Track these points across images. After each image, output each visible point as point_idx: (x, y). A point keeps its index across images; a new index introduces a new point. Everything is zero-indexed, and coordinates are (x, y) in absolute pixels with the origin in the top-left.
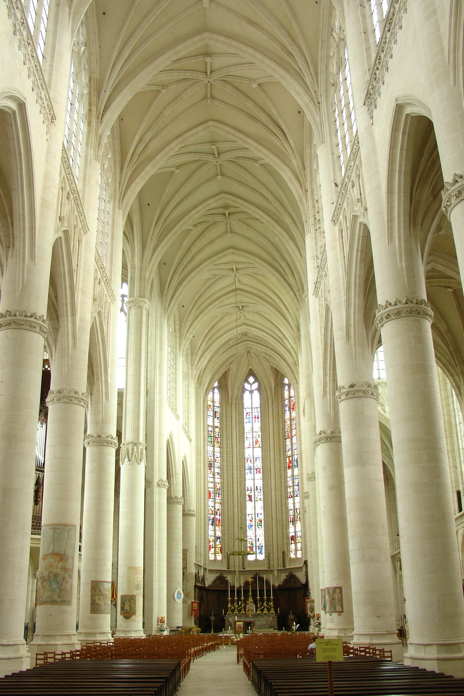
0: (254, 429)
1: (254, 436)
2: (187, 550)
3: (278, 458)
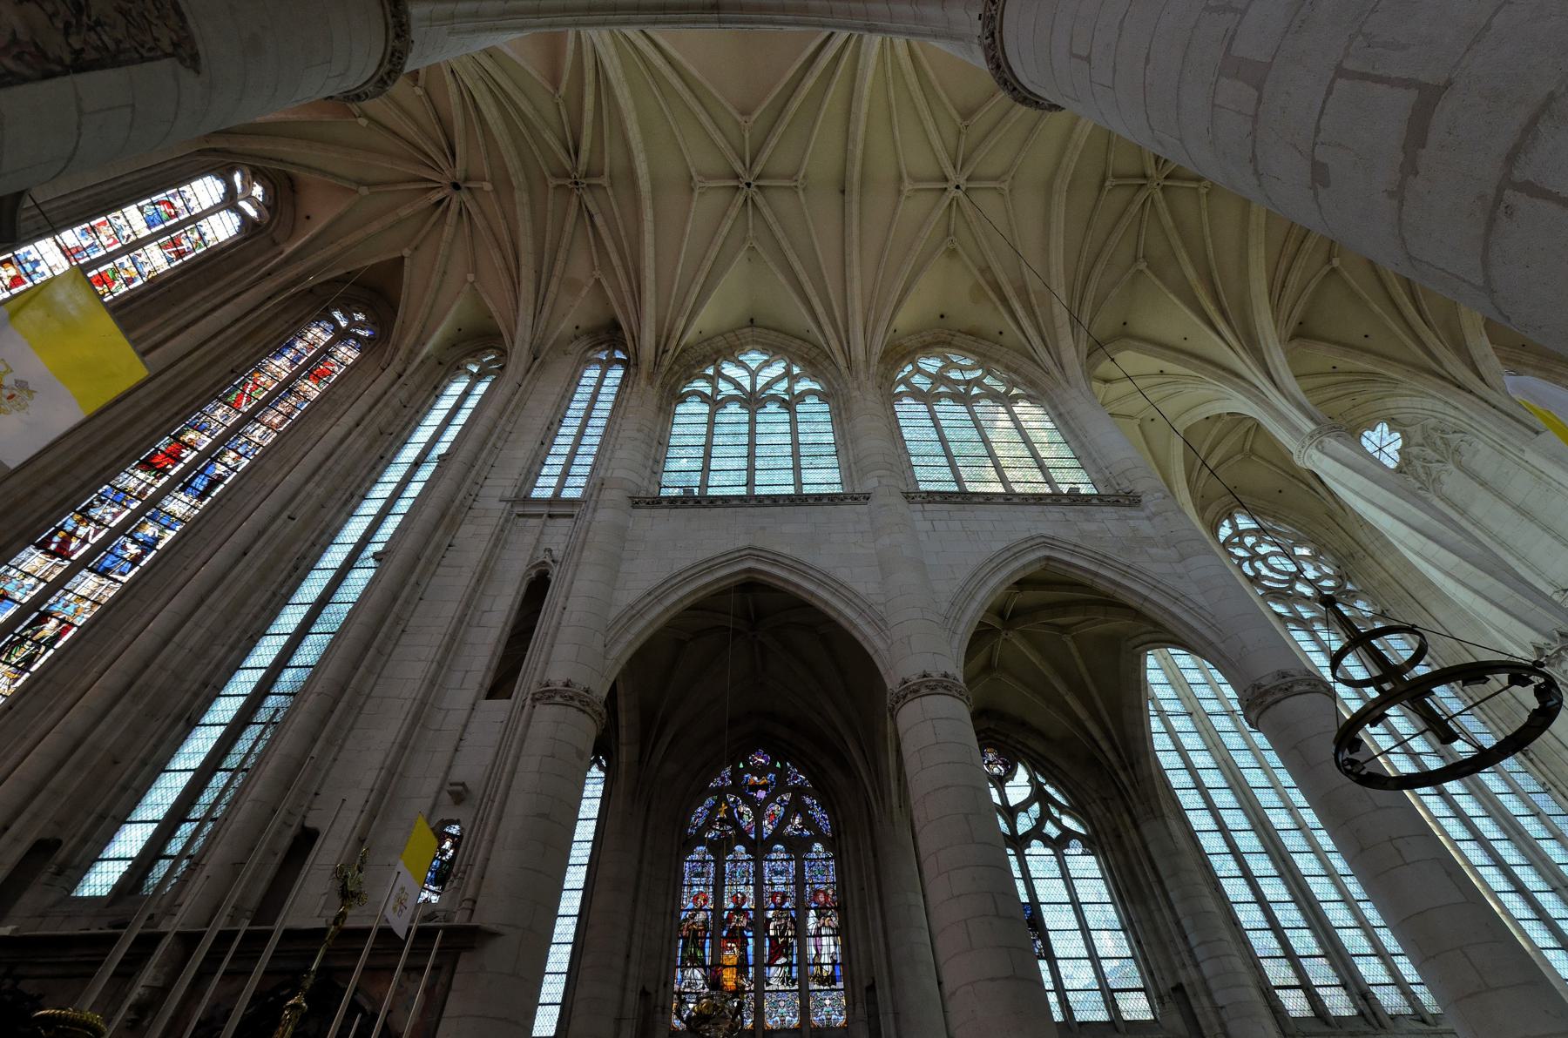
0: (140, 251)
1: (117, 262)
2: (193, 61)
3: (145, 404)
